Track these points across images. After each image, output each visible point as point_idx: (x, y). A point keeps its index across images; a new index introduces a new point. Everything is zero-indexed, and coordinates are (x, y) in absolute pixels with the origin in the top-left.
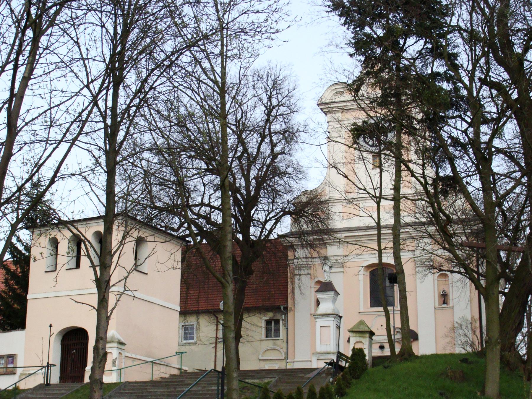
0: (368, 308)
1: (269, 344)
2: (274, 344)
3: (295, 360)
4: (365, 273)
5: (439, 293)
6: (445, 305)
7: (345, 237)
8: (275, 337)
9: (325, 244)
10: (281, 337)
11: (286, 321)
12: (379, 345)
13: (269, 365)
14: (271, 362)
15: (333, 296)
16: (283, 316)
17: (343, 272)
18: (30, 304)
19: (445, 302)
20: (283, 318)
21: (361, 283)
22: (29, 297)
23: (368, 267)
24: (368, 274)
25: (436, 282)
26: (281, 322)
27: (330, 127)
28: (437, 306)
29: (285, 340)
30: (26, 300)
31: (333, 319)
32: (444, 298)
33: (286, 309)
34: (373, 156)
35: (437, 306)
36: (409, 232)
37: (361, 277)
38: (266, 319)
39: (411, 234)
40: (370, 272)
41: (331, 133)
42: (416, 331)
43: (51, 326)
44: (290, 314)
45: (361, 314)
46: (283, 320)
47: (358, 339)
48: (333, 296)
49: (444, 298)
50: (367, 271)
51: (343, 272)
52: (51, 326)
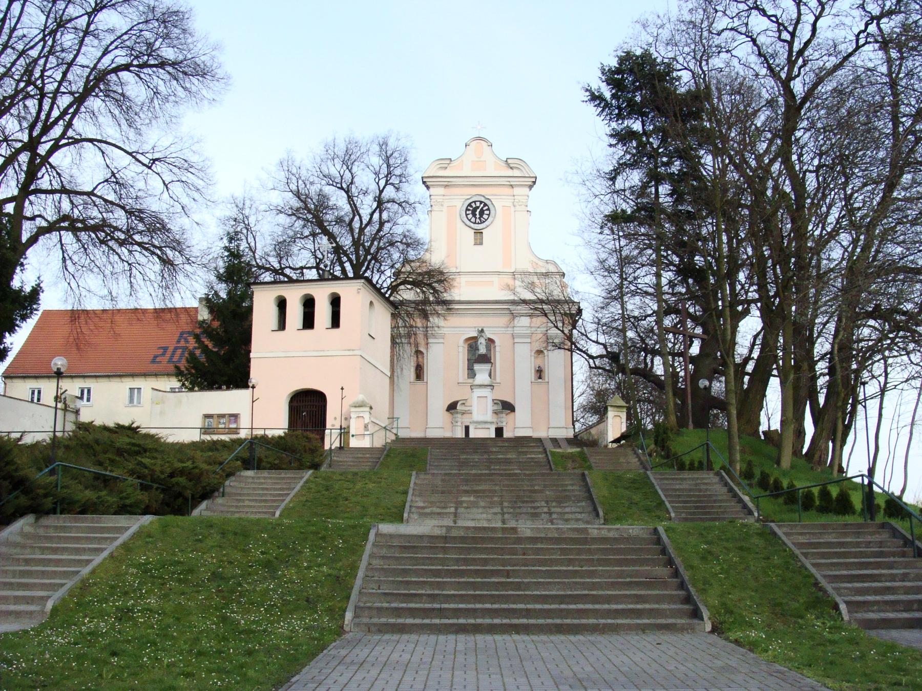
18: (252, 361)
19: (540, 378)
21: (461, 355)
22: (252, 355)
24: (466, 346)
30: (249, 360)
32: (540, 373)
37: (461, 349)
42: (512, 402)
43: (342, 389)
47: (616, 414)
49: (540, 373)
52: (342, 389)
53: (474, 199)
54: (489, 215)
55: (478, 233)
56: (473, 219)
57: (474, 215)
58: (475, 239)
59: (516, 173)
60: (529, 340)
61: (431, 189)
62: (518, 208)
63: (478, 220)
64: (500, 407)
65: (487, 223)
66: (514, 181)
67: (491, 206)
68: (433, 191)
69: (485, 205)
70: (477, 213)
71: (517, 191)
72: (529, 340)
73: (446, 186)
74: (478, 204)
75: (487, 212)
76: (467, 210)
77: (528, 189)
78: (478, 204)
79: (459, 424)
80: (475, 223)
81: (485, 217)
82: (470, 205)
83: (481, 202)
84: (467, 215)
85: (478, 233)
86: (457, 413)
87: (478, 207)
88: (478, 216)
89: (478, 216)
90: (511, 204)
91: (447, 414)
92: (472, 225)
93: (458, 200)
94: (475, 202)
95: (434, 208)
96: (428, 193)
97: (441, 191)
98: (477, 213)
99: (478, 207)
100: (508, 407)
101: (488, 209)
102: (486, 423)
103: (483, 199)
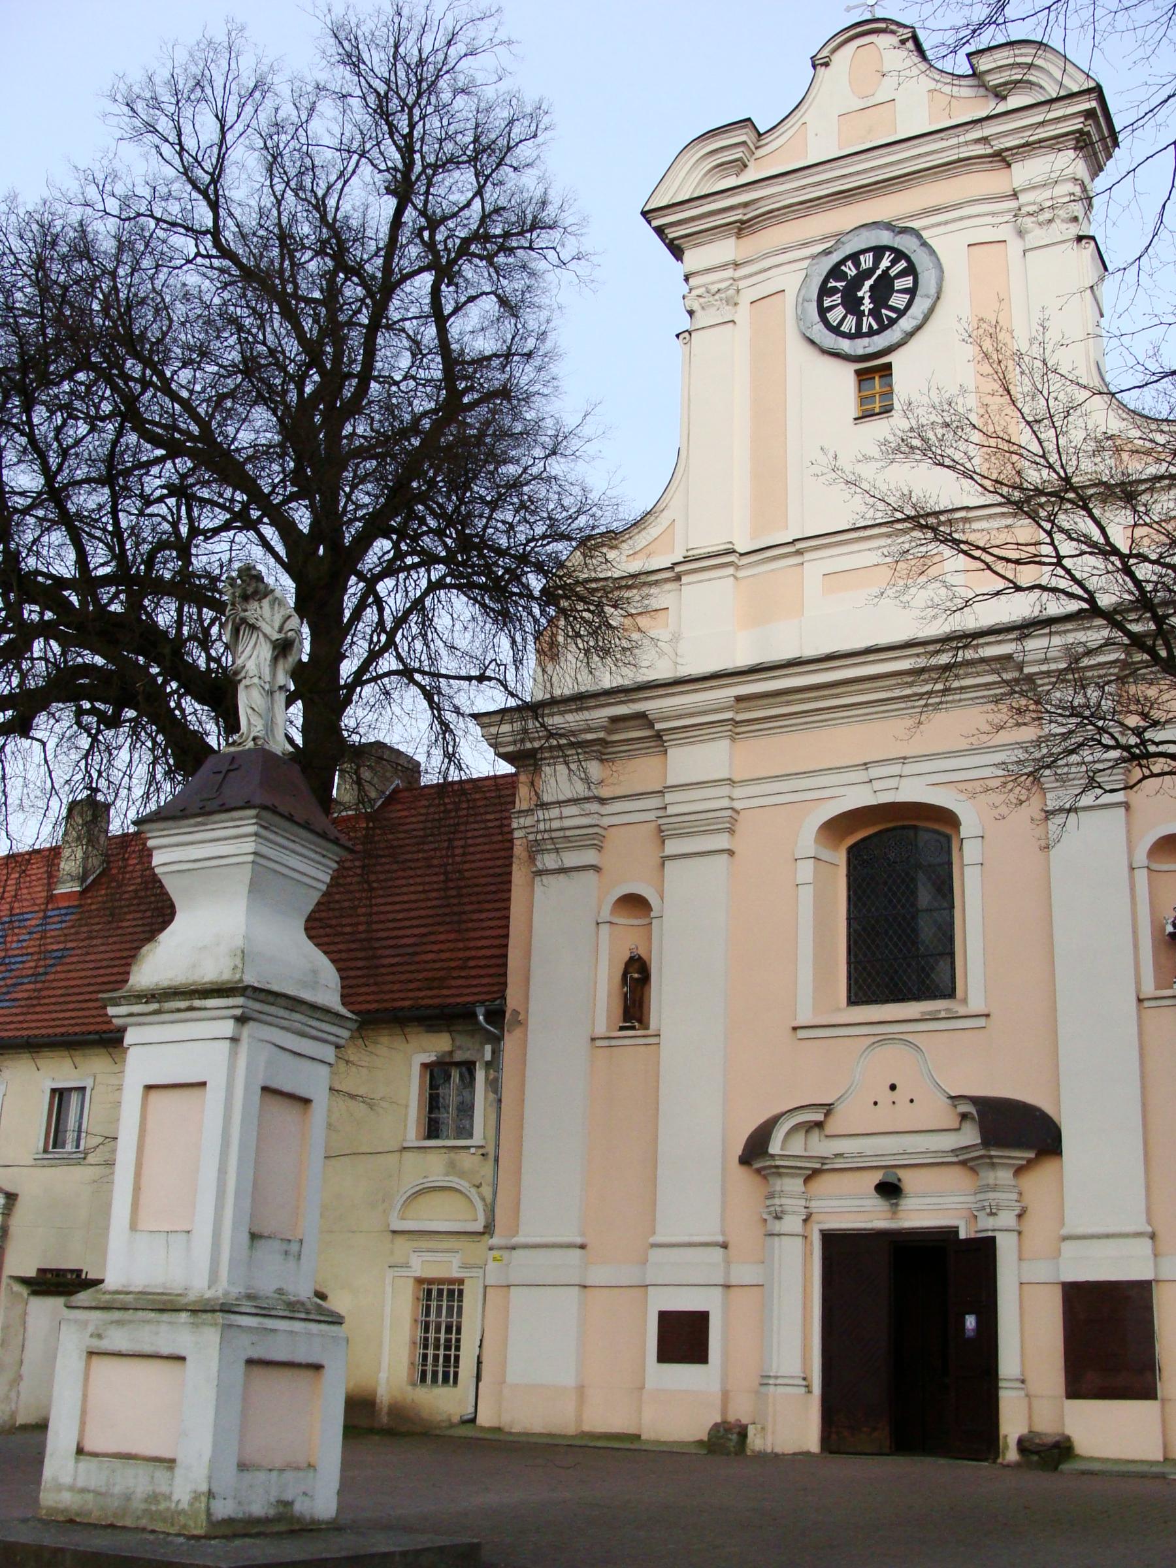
0: (839, 1010)
1: (432, 1166)
2: (452, 1167)
3: (515, 1240)
4: (826, 854)
5: (1157, 928)
7: (739, 699)
8: (457, 1138)
9: (659, 736)
10: (477, 1139)
11: (493, 1065)
12: (877, 1177)
13: (428, 1257)
14: (424, 1244)
15: (249, 846)
16: (488, 1048)
17: (731, 853)
20: (488, 1056)
21: (806, 895)
23: (837, 827)
25: (1142, 876)
26: (480, 1075)
27: (695, 293)
28: (1149, 989)
29: (490, 1149)
31: (227, 1027)
33: (497, 1016)
34: (858, 373)
35: (1149, 989)
36: (1009, 657)
37: (806, 871)
38: (430, 1058)
39: (1020, 667)
40: (850, 850)
41: (699, 314)
42: (1048, 1109)
44: (510, 1043)
45: (802, 1034)
46: (488, 1065)
48: (249, 846)
50: (836, 848)
51: (731, 853)
53: (848, 249)
54: (912, 292)
55: (874, 374)
56: (850, 324)
57: (852, 305)
58: (862, 400)
59: (1014, 102)
61: (687, 255)
63: (868, 322)
64: (970, 1136)
65: (906, 324)
66: (1005, 134)
67: (921, 259)
68: (695, 258)
69: (899, 255)
70: (864, 292)
71: (1025, 171)
73: (742, 228)
75: (907, 282)
76: (824, 291)
77: (1069, 162)
78: (867, 261)
79: (792, 1223)
80: (858, 334)
81: (899, 301)
82: (835, 272)
83: (878, 251)
84: (823, 312)
85: (874, 374)
86: (778, 1172)
87: (869, 273)
88: (867, 305)
89: (867, 305)
91: (741, 1175)
92: (845, 345)
93: (788, 267)
94: (854, 257)
95: (702, 319)
96: (679, 269)
97: (725, 249)
98: (864, 292)
99: (869, 273)
100: (1017, 1132)
101: (911, 270)
102: (165, 1305)
103: (885, 238)
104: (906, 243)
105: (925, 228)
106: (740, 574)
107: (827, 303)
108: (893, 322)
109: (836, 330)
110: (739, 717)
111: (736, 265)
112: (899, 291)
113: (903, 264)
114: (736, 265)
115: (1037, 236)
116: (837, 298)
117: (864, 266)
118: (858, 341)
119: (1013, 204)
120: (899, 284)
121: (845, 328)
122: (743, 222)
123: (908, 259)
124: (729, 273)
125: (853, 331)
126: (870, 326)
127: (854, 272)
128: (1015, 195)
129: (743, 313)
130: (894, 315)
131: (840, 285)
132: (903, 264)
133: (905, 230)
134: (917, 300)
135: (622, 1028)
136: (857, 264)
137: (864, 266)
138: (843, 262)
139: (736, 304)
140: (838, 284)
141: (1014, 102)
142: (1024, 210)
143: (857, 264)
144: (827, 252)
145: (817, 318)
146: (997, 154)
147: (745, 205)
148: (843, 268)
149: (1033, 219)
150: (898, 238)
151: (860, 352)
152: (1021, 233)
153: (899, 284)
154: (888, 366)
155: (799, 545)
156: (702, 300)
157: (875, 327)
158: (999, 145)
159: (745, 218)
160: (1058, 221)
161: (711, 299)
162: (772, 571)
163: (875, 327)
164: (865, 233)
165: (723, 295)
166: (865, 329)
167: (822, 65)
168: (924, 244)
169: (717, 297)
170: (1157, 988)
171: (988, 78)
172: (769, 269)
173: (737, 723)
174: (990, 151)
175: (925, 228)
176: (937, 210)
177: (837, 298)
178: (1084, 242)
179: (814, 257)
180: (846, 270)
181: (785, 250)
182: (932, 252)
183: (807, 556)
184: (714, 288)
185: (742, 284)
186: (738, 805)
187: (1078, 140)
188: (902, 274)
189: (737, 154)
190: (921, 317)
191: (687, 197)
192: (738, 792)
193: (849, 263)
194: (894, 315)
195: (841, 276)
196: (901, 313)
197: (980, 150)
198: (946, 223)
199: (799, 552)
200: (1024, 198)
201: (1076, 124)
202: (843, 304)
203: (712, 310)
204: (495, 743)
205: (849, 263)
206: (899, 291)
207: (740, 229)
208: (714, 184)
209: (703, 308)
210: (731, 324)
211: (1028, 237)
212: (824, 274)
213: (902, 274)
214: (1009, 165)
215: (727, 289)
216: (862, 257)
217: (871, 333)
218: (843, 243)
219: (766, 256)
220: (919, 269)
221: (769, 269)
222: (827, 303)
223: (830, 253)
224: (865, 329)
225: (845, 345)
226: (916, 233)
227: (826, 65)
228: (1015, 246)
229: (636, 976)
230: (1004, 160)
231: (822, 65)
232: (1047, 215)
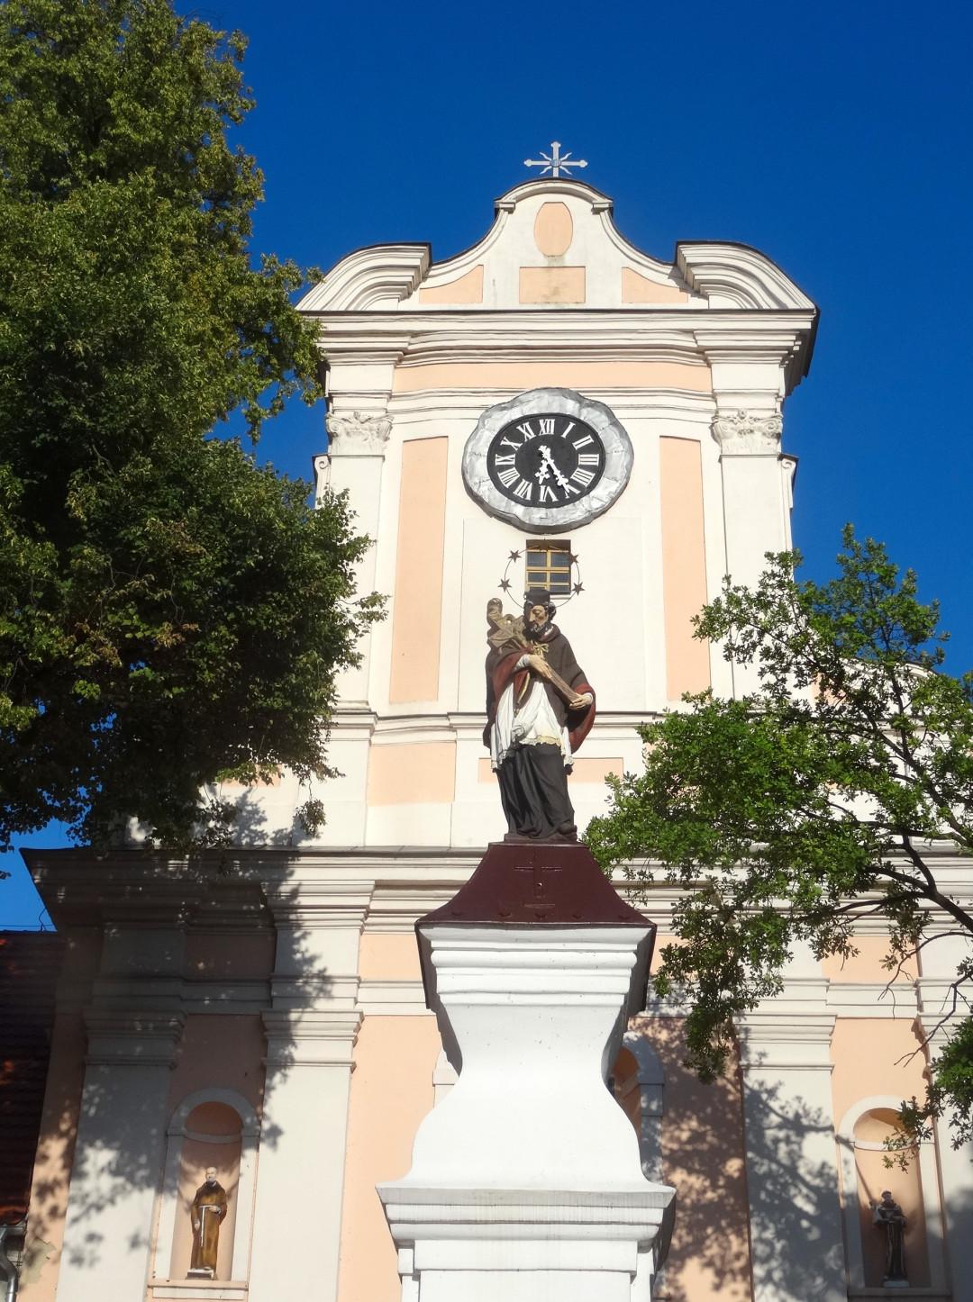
6: (899, 1286)
7: (380, 885)
34: (530, 544)
54: (599, 471)
56: (525, 489)
60: (821, 1055)
62: (734, 443)
66: (712, 332)
69: (583, 428)
71: (726, 374)
72: (821, 1055)
73: (402, 357)
74: (548, 427)
75: (593, 459)
76: (496, 448)
78: (548, 427)
80: (534, 502)
81: (584, 477)
82: (510, 430)
84: (493, 471)
90: (703, 433)
92: (519, 510)
94: (534, 420)
97: (380, 375)
101: (598, 447)
103: (570, 407)
104: (587, 415)
105: (619, 407)
106: (375, 739)
107: (499, 461)
108: (574, 498)
109: (508, 493)
110: (375, 905)
111: (391, 396)
112: (582, 467)
113: (588, 440)
114: (391, 396)
115: (734, 443)
116: (511, 459)
117: (543, 432)
118: (534, 510)
119: (712, 405)
120: (585, 459)
121: (518, 492)
122: (406, 352)
123: (595, 435)
124: (382, 403)
125: (528, 498)
126: (549, 497)
127: (533, 436)
128: (714, 396)
129: (394, 449)
130: (577, 492)
131: (516, 445)
132: (588, 440)
133: (594, 405)
134: (603, 481)
135: (191, 1276)
136: (536, 428)
137: (543, 432)
138: (521, 421)
139: (386, 439)
140: (513, 444)
141: (718, 301)
142: (721, 413)
143: (536, 428)
144: (501, 407)
145: (487, 476)
146: (701, 352)
147: (415, 334)
148: (519, 428)
149: (732, 425)
150: (585, 411)
151: (537, 522)
152: (716, 437)
153: (585, 459)
154: (566, 545)
155: (454, 720)
156: (347, 424)
157: (554, 499)
158: (704, 341)
159: (411, 348)
160: (758, 435)
161: (359, 426)
162: (417, 743)
163: (554, 499)
164: (546, 396)
165: (375, 426)
166: (542, 499)
167: (505, 209)
168: (615, 423)
169: (367, 425)
170: (867, 1285)
171: (695, 271)
172: (430, 409)
173: (369, 912)
174: (695, 345)
175: (619, 407)
176: (627, 392)
177: (511, 459)
178: (785, 461)
179: (488, 409)
180: (524, 432)
181: (452, 394)
182: (623, 434)
183: (462, 734)
184: (364, 415)
185: (398, 418)
186: (367, 1010)
187: (785, 357)
188: (587, 450)
189: (407, 276)
190: (607, 500)
191: (342, 308)
192: (363, 994)
193: (527, 424)
194: (577, 492)
195: (518, 437)
196: (586, 491)
197: (687, 342)
198: (638, 407)
199: (451, 728)
200: (722, 401)
201: (789, 341)
202: (519, 466)
203: (361, 438)
204: (45, 891)
205: (527, 425)
206: (582, 467)
207: (400, 361)
208: (371, 303)
209: (348, 434)
210: (381, 459)
211: (725, 443)
212: (498, 430)
213: (587, 450)
214: (709, 366)
215: (380, 419)
216: (541, 421)
217: (549, 504)
218: (521, 402)
219: (429, 394)
220: (608, 450)
221: (430, 409)
222: (499, 461)
223: (505, 408)
224: (542, 499)
225: (519, 510)
226: (608, 411)
227: (511, 211)
228: (710, 449)
229: (215, 1208)
230: (706, 360)
231: (505, 209)
232: (746, 425)
